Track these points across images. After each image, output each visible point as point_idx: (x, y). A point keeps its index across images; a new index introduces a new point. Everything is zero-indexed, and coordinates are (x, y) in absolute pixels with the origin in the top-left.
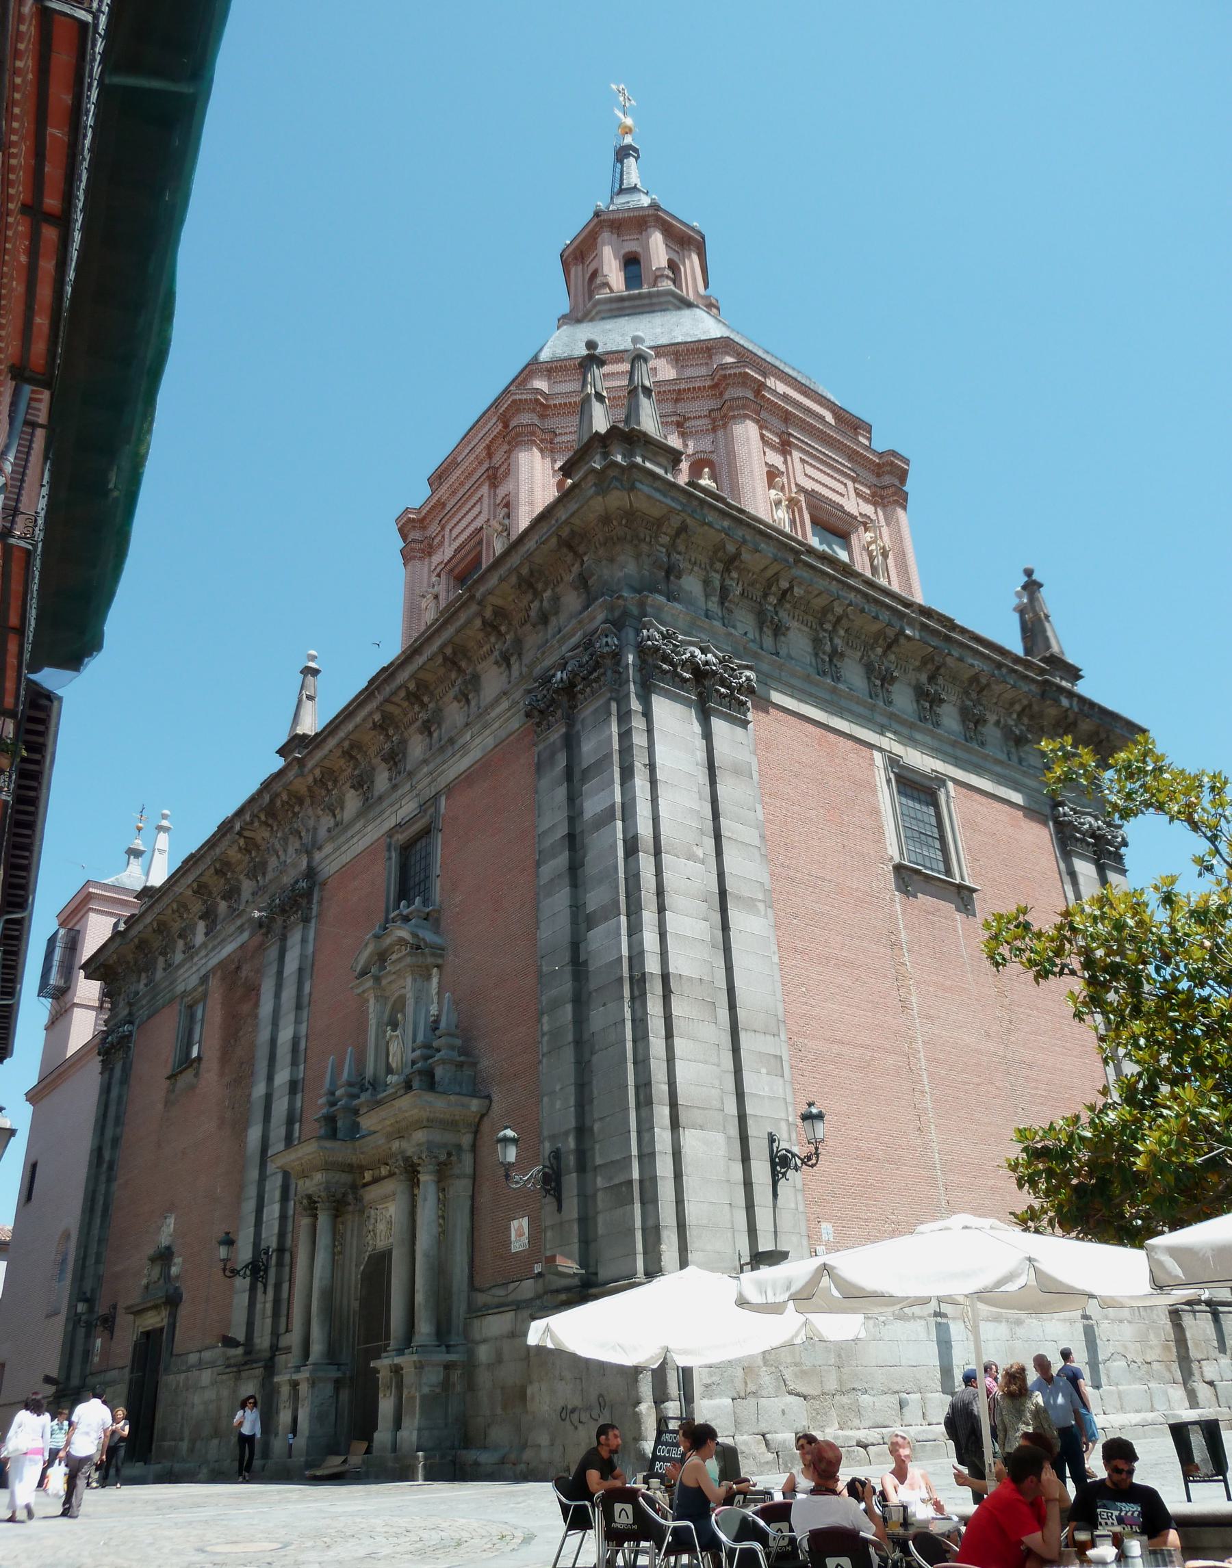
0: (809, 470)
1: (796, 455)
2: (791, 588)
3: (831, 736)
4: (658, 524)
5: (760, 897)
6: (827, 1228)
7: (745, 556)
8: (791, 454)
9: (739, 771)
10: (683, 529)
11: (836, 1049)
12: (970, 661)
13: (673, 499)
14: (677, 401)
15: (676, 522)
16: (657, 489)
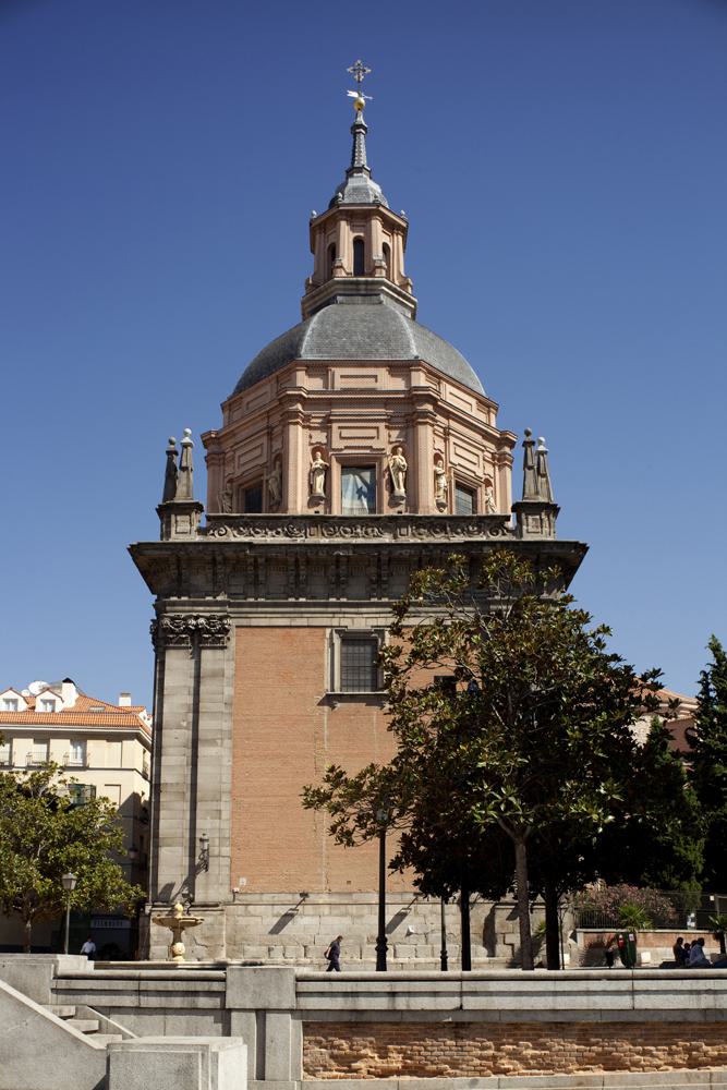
0: (345, 433)
1: (335, 426)
2: (256, 561)
3: (293, 631)
4: (167, 560)
5: (219, 736)
6: (243, 881)
7: (219, 558)
8: (331, 427)
9: (218, 674)
10: (179, 560)
11: (263, 800)
12: (399, 552)
13: (166, 549)
14: (268, 417)
15: (173, 560)
16: (156, 549)
